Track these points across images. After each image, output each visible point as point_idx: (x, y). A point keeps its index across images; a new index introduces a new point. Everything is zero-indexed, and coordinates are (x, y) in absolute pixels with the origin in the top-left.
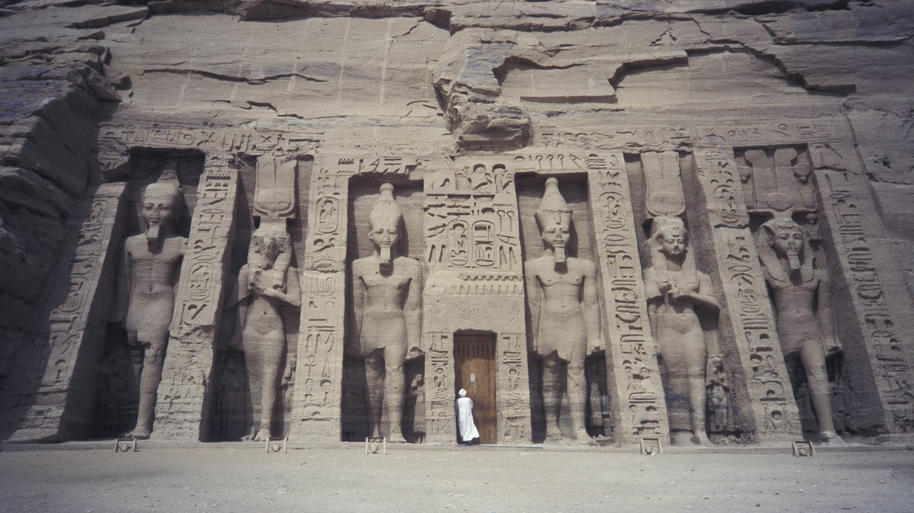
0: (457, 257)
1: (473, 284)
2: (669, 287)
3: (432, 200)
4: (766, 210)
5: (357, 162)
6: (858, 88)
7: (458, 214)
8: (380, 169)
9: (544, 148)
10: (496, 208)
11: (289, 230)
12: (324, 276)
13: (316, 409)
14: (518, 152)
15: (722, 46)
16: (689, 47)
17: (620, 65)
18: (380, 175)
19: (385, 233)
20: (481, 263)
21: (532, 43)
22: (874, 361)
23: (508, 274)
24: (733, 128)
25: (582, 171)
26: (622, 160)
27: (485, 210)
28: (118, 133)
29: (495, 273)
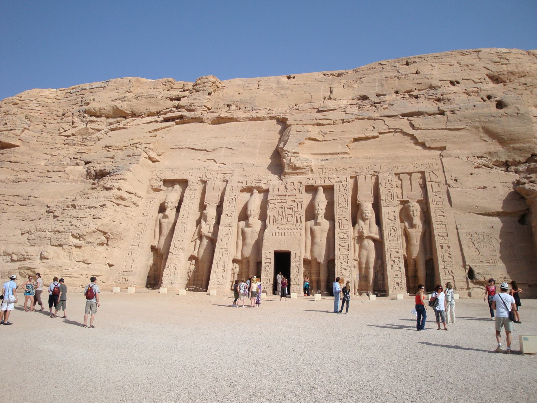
1: (283, 232)
2: (363, 232)
4: (407, 199)
5: (245, 182)
6: (447, 148)
8: (253, 185)
9: (318, 175)
10: (296, 200)
11: (217, 210)
12: (227, 229)
13: (219, 280)
14: (307, 176)
15: (393, 130)
16: (380, 131)
17: (352, 140)
18: (252, 187)
19: (252, 211)
21: (317, 131)
22: (440, 262)
23: (296, 227)
24: (395, 165)
25: (331, 184)
26: (349, 179)
27: (292, 201)
28: (159, 174)
29: (292, 228)
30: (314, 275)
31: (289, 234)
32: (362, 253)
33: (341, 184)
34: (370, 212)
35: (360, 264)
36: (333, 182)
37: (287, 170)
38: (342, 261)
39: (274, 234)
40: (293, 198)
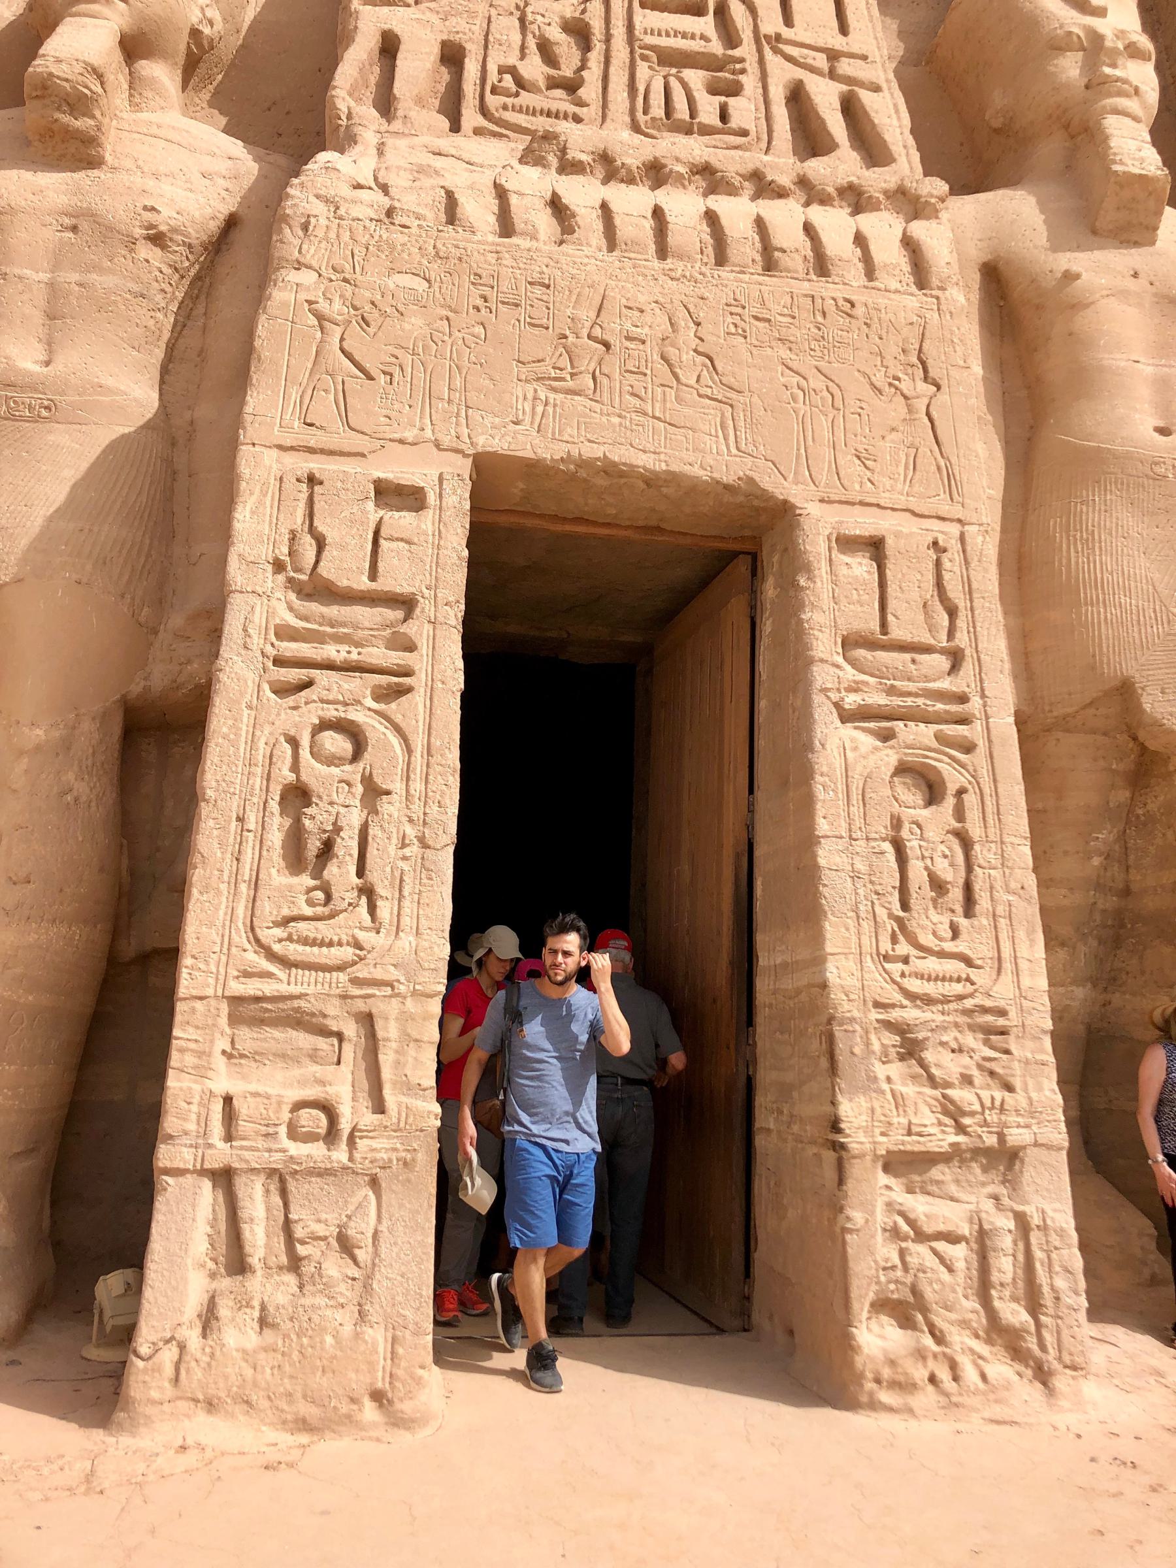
0: (526, 98)
39: (479, 211)
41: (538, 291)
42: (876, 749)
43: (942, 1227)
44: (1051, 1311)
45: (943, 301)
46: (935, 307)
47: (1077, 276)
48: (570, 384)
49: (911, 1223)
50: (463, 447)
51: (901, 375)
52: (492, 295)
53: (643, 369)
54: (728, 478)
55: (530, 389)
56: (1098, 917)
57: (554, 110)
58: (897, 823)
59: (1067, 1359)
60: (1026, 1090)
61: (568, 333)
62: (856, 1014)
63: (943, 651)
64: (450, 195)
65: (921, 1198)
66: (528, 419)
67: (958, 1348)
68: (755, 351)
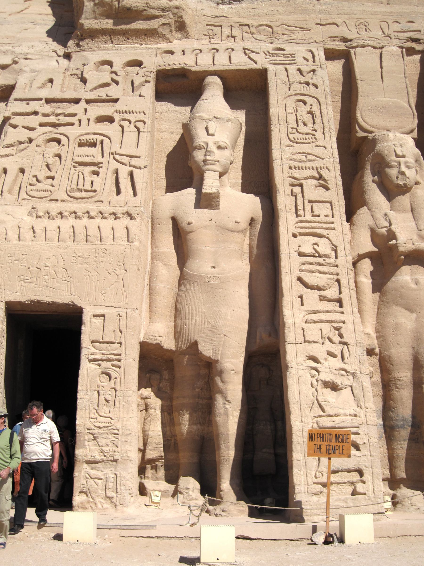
1: (52, 225)
3: (22, 107)
7: (54, 125)
10: (117, 117)
20: (78, 194)
23: (112, 210)
26: (321, 55)
27: (101, 119)
30: (186, 417)
31: (80, 237)
32: (390, 321)
33: (292, 69)
34: (410, 160)
35: (385, 366)
36: (262, 62)
37: (87, 21)
38: (319, 351)
39: (13, 235)
40: (106, 110)
41: (24, 256)
42: (96, 369)
43: (96, 476)
44: (119, 493)
45: (132, 246)
46: (129, 248)
47: (192, 223)
48: (30, 280)
49: (89, 475)
50: (3, 300)
51: (117, 269)
52: (13, 259)
53: (49, 275)
54: (67, 302)
55: (20, 283)
56: (200, 406)
57: (44, 190)
58: (99, 387)
59: (121, 503)
60: (121, 447)
61: (31, 267)
62: (82, 431)
63: (118, 343)
64: (6, 230)
65: (94, 471)
66: (19, 291)
67: (97, 501)
68: (78, 266)
